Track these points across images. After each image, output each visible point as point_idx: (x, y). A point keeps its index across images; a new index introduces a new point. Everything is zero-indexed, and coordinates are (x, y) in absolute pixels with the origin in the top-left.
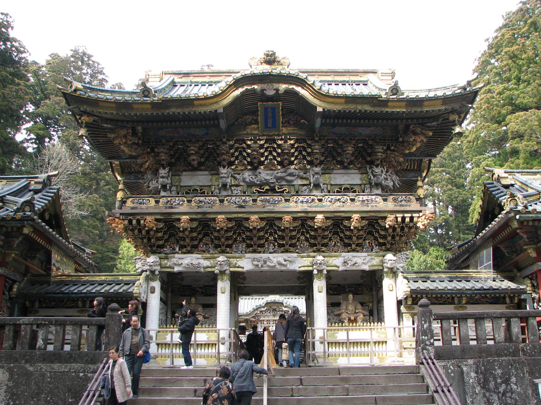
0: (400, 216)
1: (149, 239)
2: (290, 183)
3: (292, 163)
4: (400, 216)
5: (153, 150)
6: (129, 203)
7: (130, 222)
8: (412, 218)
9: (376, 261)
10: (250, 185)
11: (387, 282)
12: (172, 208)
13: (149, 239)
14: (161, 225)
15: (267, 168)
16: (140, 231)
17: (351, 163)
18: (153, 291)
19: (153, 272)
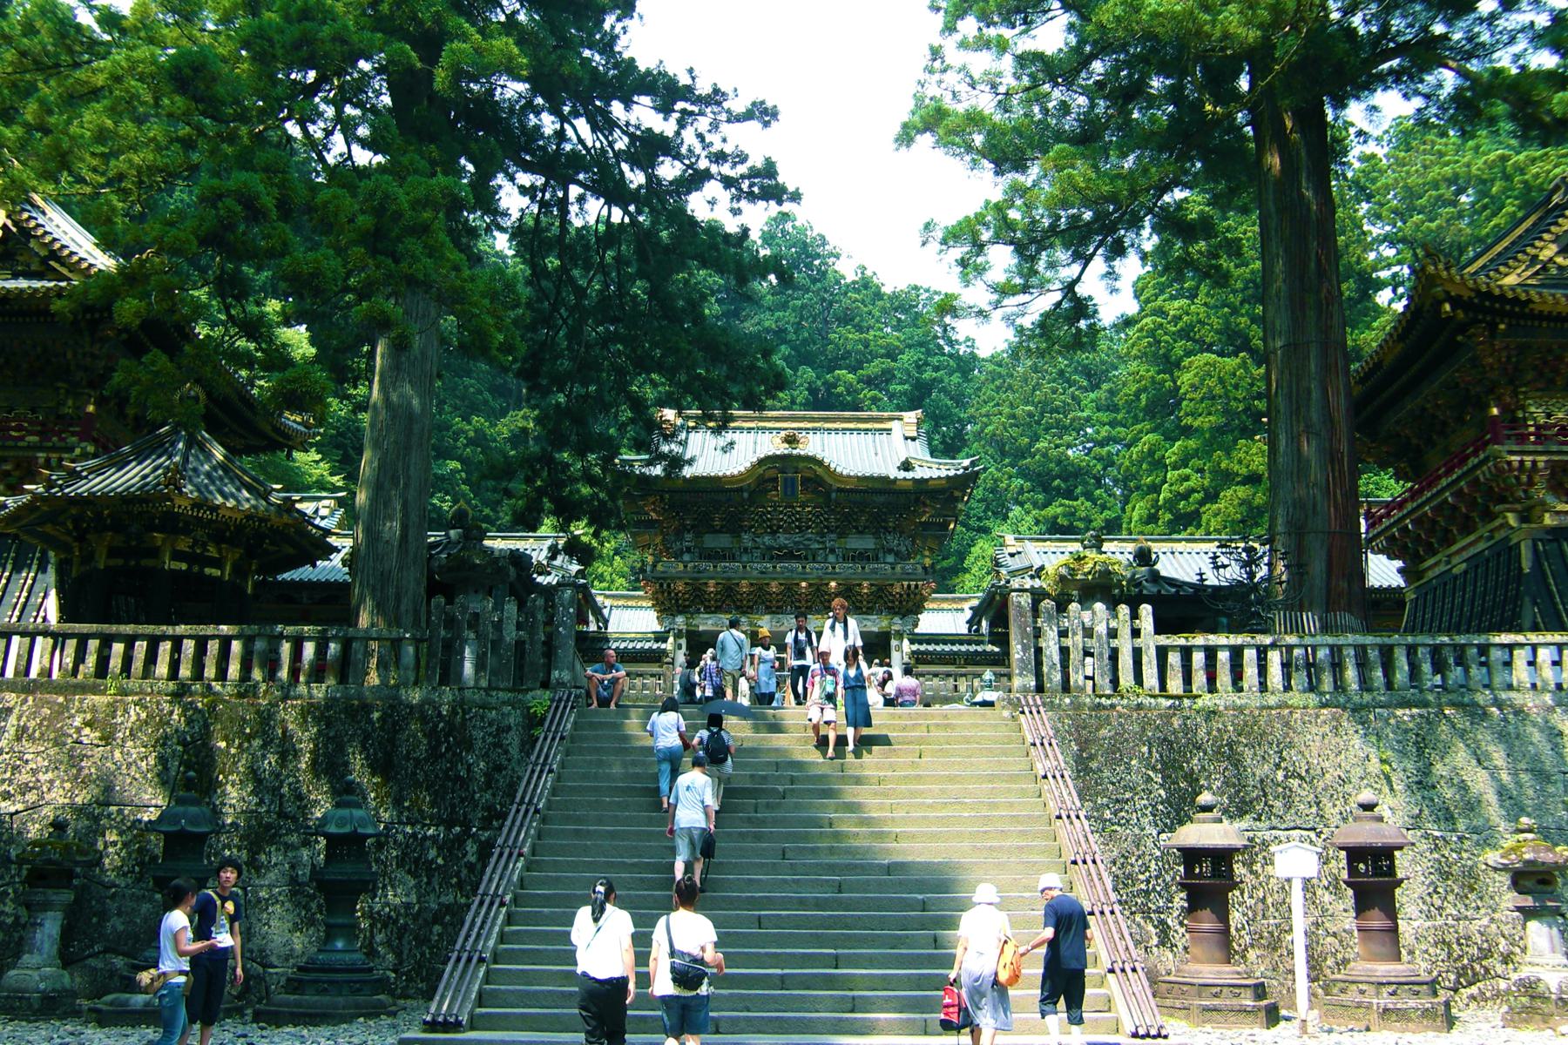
0: (906, 583)
1: (677, 600)
2: (807, 548)
3: (809, 527)
4: (906, 583)
5: (678, 514)
6: (659, 567)
7: (661, 585)
8: (917, 586)
9: (885, 623)
10: (770, 548)
11: (894, 643)
12: (699, 572)
13: (677, 600)
14: (689, 588)
15: (786, 532)
16: (669, 593)
17: (865, 527)
18: (680, 647)
19: (680, 631)
